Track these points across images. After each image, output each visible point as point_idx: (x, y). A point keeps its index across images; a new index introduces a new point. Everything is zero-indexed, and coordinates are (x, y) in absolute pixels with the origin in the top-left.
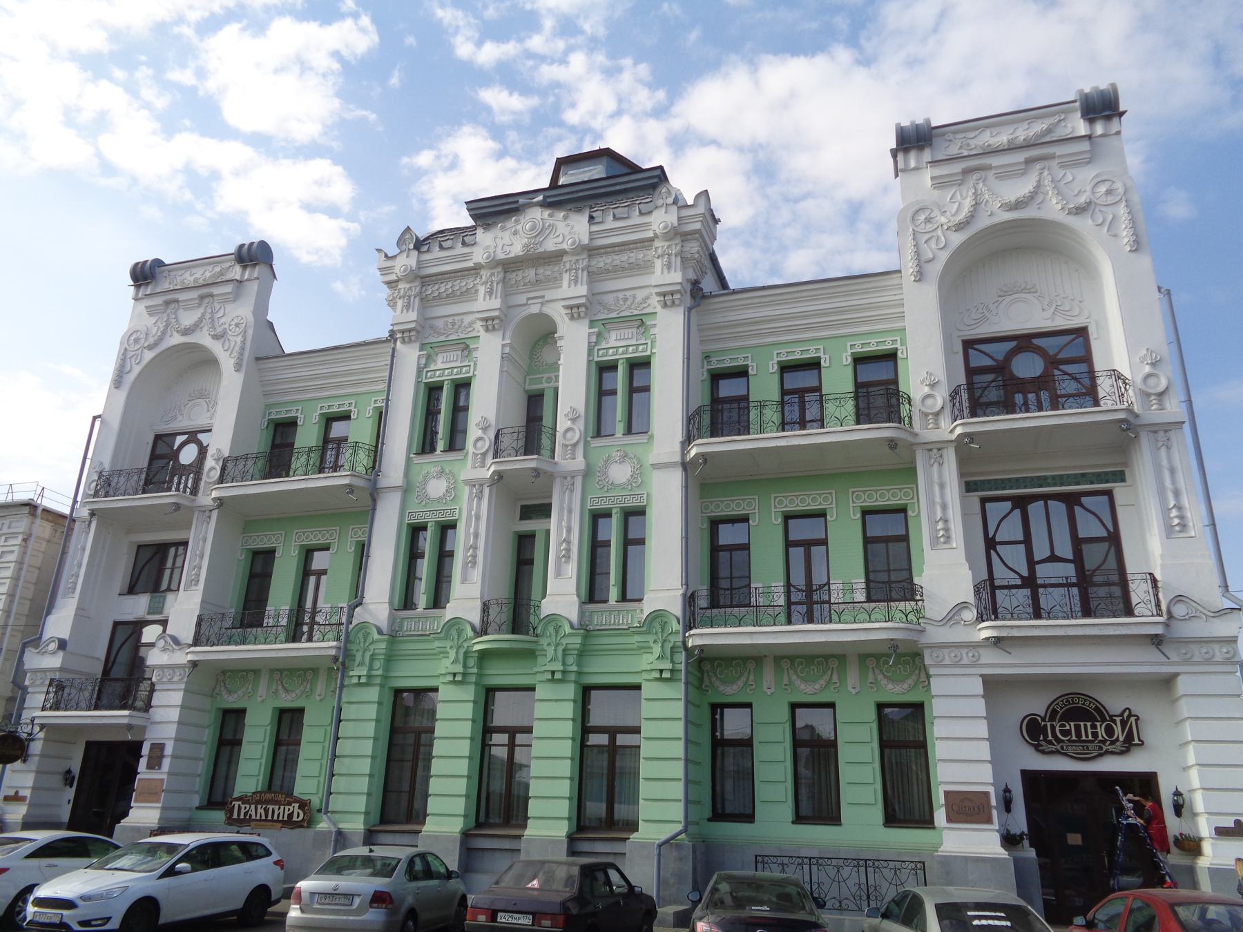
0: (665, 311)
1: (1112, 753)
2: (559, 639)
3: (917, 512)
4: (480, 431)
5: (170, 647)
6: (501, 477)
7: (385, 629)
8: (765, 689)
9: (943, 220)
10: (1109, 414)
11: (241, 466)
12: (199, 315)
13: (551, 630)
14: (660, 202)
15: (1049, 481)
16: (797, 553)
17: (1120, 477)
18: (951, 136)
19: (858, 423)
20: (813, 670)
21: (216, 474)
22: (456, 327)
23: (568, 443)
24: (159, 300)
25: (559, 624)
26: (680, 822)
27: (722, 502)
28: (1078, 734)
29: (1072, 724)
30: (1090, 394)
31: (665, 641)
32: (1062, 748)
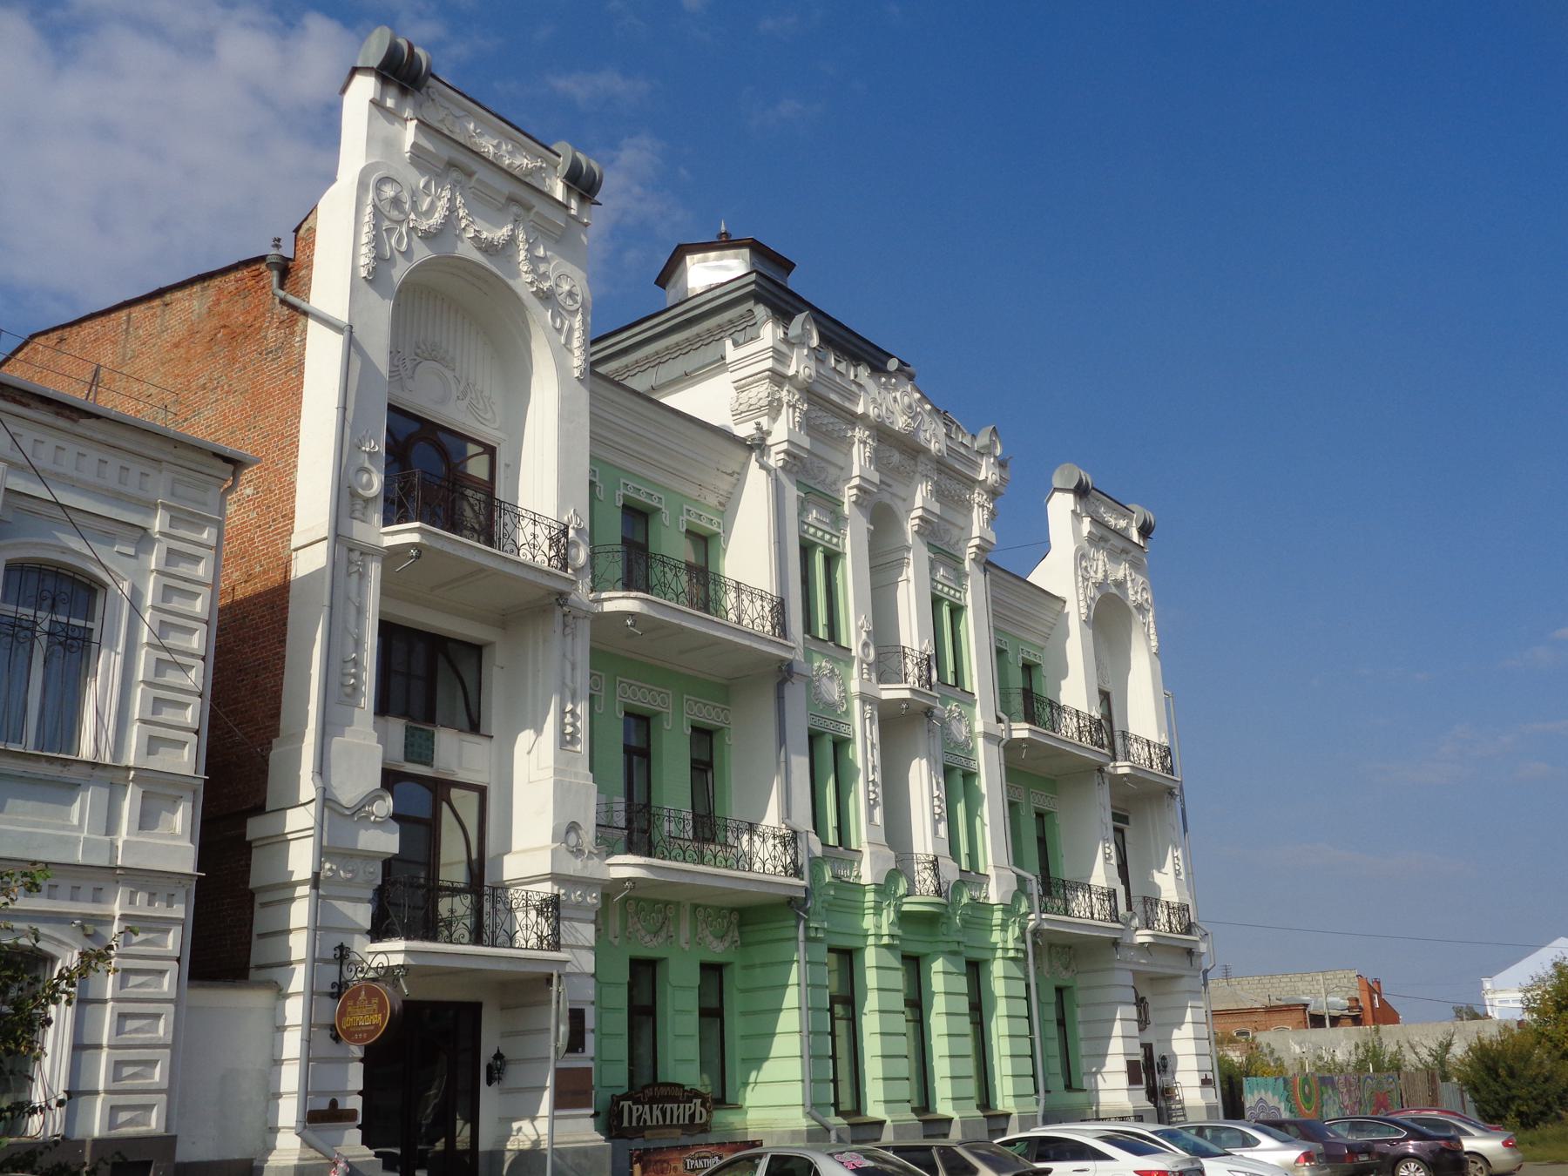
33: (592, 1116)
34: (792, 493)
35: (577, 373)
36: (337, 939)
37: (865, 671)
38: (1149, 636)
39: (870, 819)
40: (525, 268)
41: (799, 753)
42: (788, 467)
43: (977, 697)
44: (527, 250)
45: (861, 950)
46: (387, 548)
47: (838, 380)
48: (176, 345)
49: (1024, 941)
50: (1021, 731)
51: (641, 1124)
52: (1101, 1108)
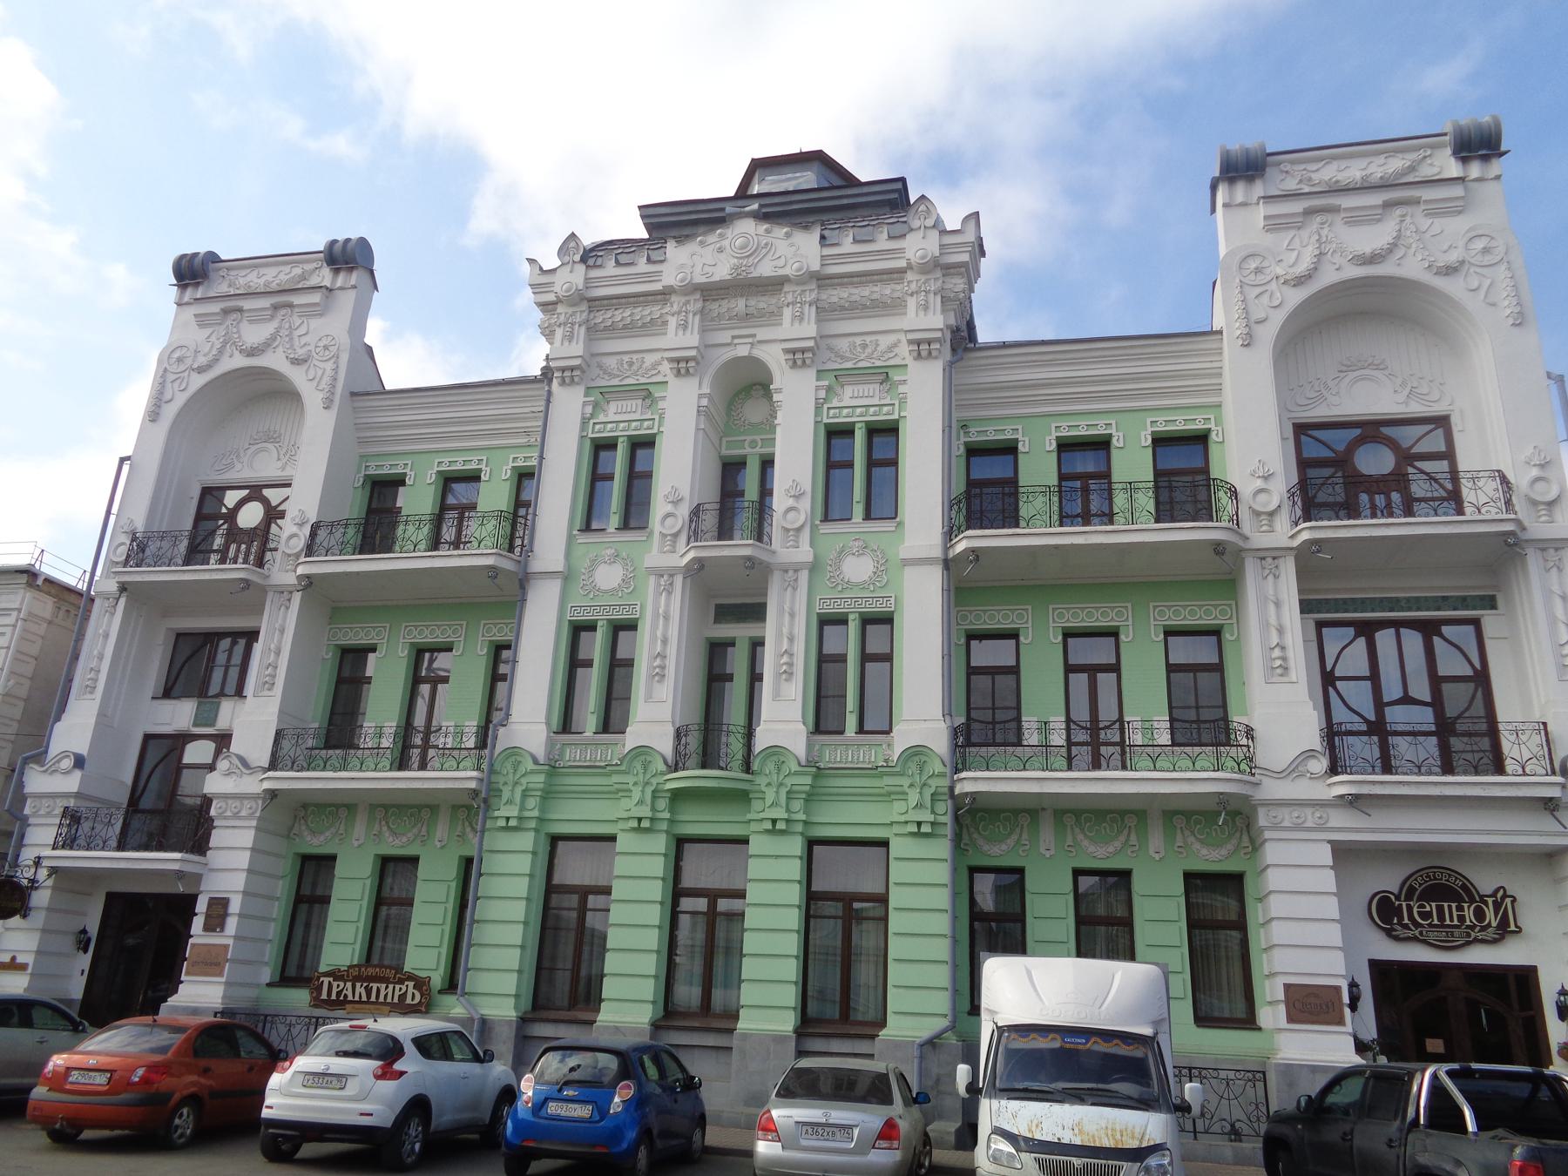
0: (919, 365)
1: (1483, 941)
2: (781, 777)
3: (1236, 634)
4: (670, 505)
5: (237, 771)
6: (702, 567)
7: (541, 758)
8: (1042, 850)
9: (1279, 271)
10: (1494, 524)
11: (338, 535)
12: (272, 330)
13: (770, 766)
14: (916, 223)
15: (1403, 604)
16: (1079, 681)
17: (1490, 603)
18: (1289, 167)
19: (1157, 521)
20: (1105, 828)
21: (300, 543)
22: (635, 368)
23: (789, 526)
24: (215, 308)
25: (782, 759)
26: (946, 1016)
27: (985, 611)
28: (1441, 917)
29: (1433, 904)
30: (1454, 499)
31: (925, 785)
32: (1421, 933)
51: (342, 998)
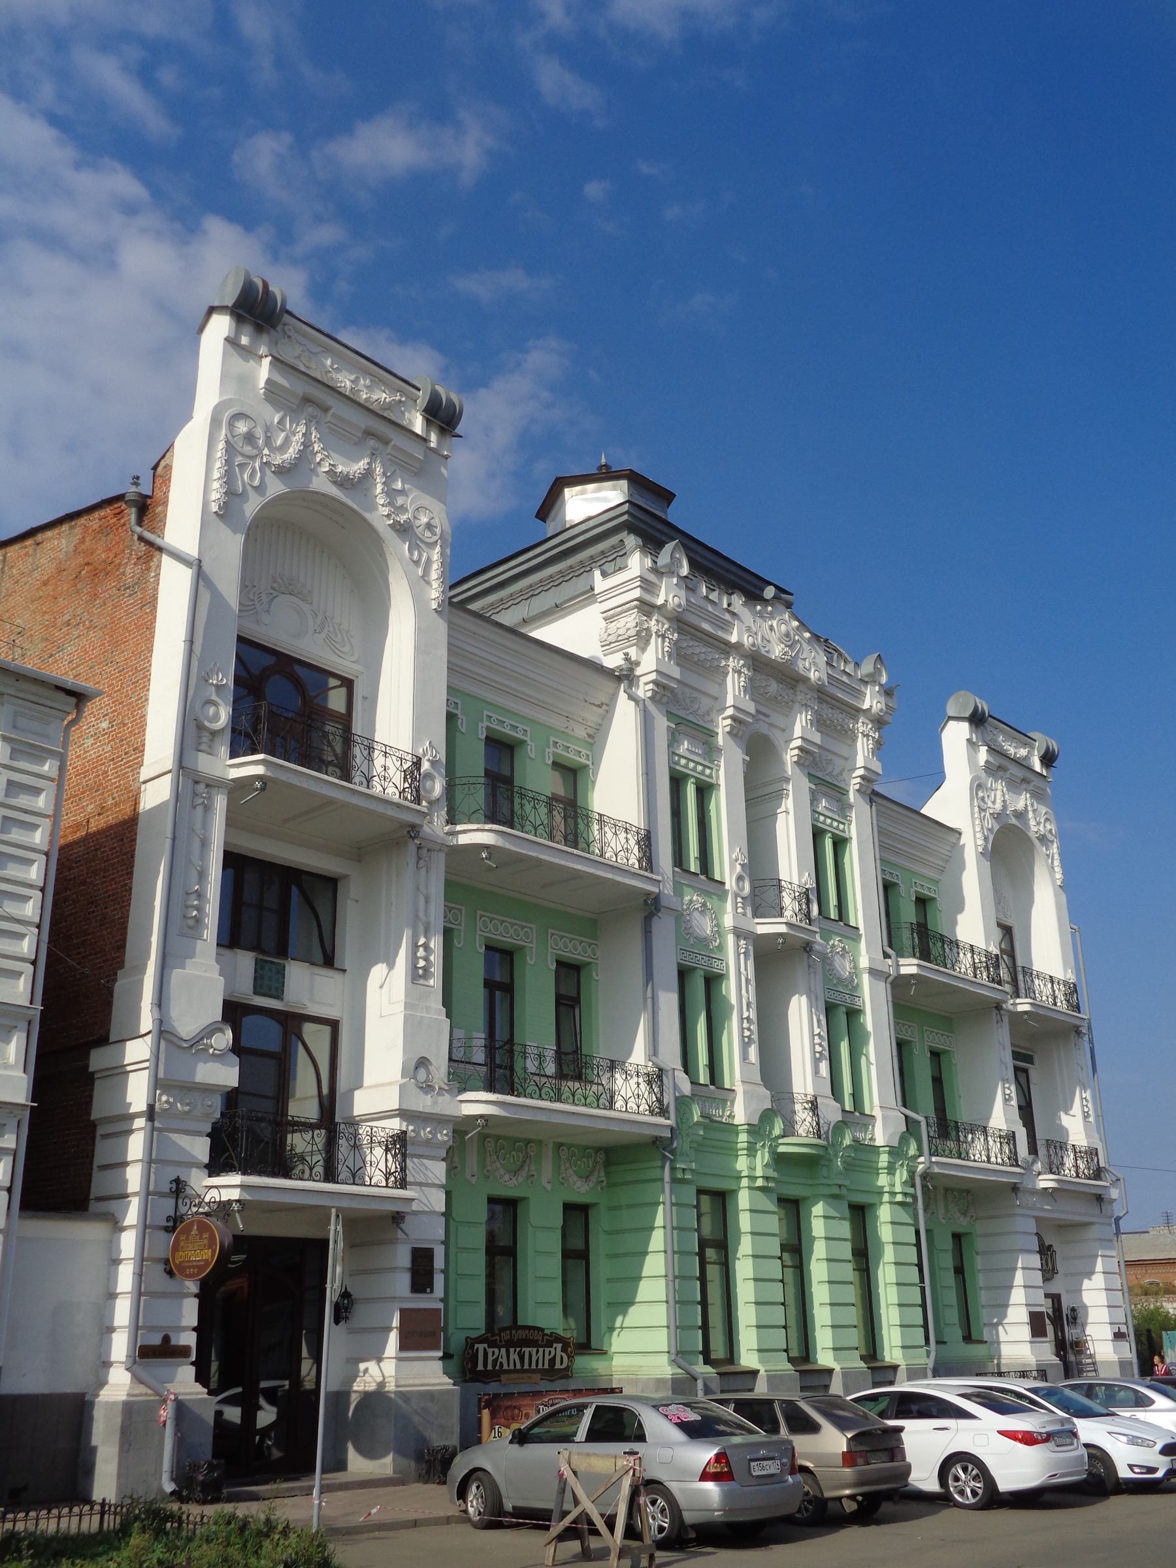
33: (440, 1359)
34: (662, 724)
35: (434, 605)
36: (172, 1173)
37: (739, 905)
38: (1053, 868)
39: (745, 1057)
40: (381, 502)
41: (668, 990)
42: (658, 697)
43: (862, 931)
44: (384, 483)
45: (734, 1192)
46: (234, 780)
47: (710, 609)
48: (45, 583)
49: (913, 1186)
50: (909, 966)
51: (497, 1368)
52: (1003, 1361)
